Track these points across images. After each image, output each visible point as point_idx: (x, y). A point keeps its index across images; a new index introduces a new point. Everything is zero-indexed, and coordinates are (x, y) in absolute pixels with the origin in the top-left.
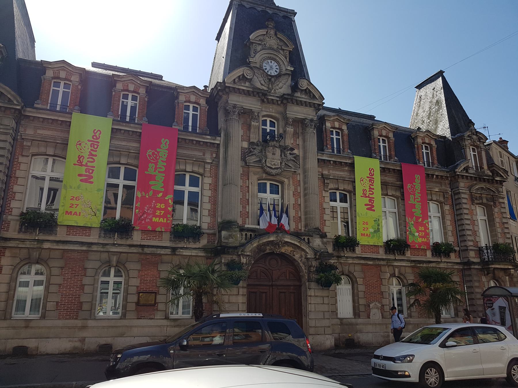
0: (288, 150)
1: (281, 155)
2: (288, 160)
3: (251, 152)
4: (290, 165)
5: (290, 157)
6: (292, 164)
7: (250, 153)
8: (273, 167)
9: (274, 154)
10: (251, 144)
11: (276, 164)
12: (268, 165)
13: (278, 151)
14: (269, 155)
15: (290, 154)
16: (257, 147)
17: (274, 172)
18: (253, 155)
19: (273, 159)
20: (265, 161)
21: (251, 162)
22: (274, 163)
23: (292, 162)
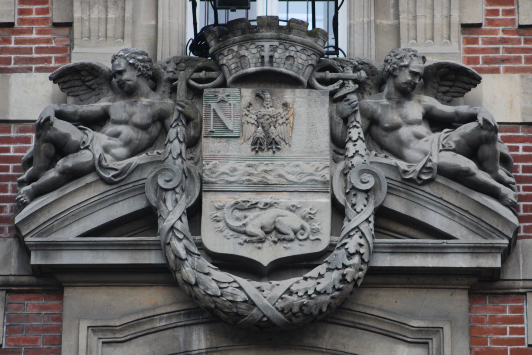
0: (405, 93)
1: (338, 144)
2: (410, 184)
3: (61, 148)
4: (436, 219)
5: (431, 148)
6: (450, 211)
7: (51, 163)
8: (265, 255)
9: (266, 144)
10: (77, 79)
11: (290, 222)
13: (307, 115)
14: (227, 159)
15: (435, 122)
16: (118, 108)
17: (268, 296)
18: (72, 175)
19: (264, 187)
20: (194, 213)
21: (71, 234)
22: (267, 217)
23: (451, 193)
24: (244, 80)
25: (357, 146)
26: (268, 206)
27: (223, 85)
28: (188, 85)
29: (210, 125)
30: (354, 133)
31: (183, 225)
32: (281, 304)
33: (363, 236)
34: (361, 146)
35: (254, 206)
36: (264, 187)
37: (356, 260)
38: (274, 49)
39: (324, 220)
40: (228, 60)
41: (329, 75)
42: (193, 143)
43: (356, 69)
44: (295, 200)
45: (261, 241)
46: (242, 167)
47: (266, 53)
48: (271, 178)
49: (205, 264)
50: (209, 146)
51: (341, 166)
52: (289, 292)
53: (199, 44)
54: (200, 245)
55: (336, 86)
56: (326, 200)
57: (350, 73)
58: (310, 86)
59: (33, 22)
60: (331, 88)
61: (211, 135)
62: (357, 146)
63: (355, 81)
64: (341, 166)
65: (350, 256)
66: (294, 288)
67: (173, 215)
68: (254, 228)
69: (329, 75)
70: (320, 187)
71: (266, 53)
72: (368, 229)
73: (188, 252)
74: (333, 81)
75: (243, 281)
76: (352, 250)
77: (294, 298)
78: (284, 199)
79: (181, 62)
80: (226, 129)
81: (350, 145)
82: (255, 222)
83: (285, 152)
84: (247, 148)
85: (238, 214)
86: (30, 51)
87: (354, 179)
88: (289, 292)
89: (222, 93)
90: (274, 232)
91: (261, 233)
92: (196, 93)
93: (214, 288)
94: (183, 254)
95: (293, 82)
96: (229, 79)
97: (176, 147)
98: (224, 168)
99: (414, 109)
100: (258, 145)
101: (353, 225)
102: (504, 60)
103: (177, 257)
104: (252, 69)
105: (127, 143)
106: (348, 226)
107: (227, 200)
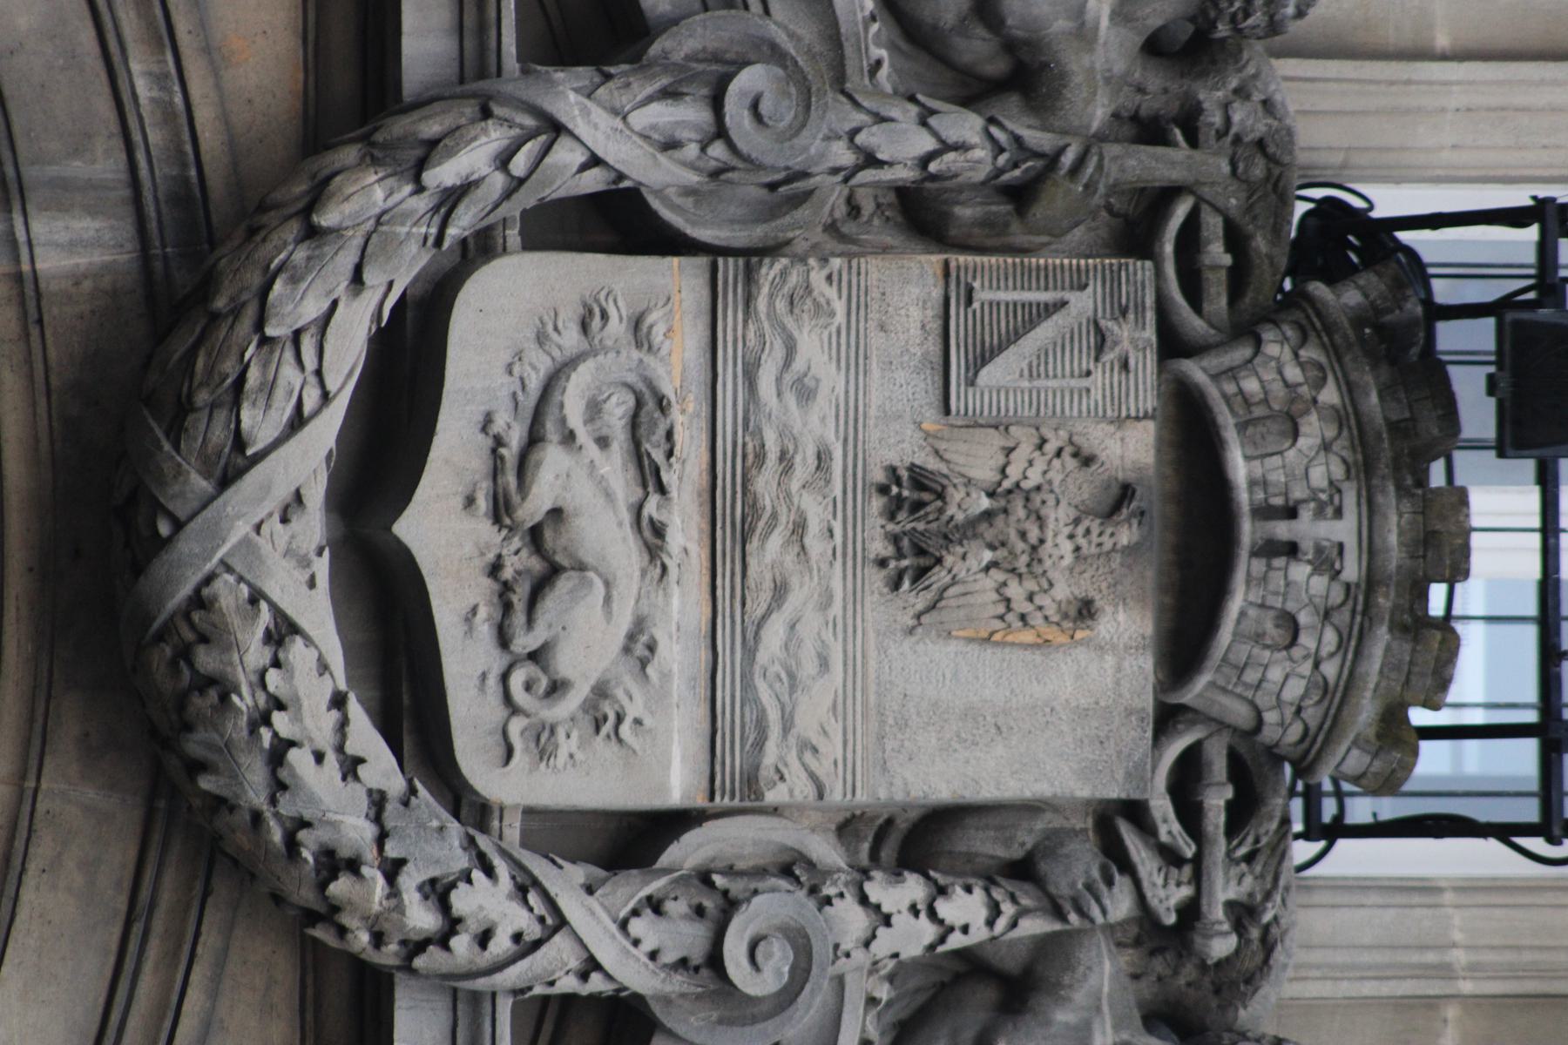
1: (920, 840)
8: (440, 529)
9: (919, 526)
11: (584, 635)
12: (504, 319)
14: (855, 359)
17: (265, 541)
19: (733, 523)
20: (618, 221)
22: (602, 532)
24: (1192, 432)
25: (908, 921)
26: (653, 536)
27: (1172, 344)
28: (1167, 195)
29: (996, 286)
30: (965, 909)
31: (565, 172)
32: (229, 594)
33: (525, 946)
34: (911, 937)
35: (650, 478)
36: (733, 523)
37: (421, 918)
38: (1327, 560)
39: (591, 781)
40: (1280, 362)
41: (1217, 800)
42: (921, 214)
43: (1242, 914)
44: (679, 656)
45: (501, 510)
46: (816, 425)
47: (1307, 529)
48: (770, 551)
49: (402, 270)
50: (908, 285)
51: (825, 850)
52: (283, 631)
53: (1350, 240)
54: (481, 248)
55: (1169, 827)
56: (677, 785)
57: (1224, 888)
58: (1167, 718)
60: (1162, 807)
61: (955, 294)
62: (908, 921)
63: (1190, 912)
64: (825, 850)
65: (438, 892)
66: (297, 652)
67: (613, 129)
69: (1217, 800)
70: (734, 761)
71: (1307, 529)
72: (554, 965)
73: (453, 197)
75: (326, 430)
76: (461, 901)
77: (256, 654)
78: (682, 608)
79: (1268, 161)
80: (983, 357)
81: (914, 888)
82: (582, 484)
83: (883, 611)
84: (897, 445)
85: (617, 410)
87: (770, 907)
88: (283, 631)
89: (1136, 338)
90: (540, 565)
91: (533, 508)
92: (1135, 225)
93: (297, 306)
94: (444, 174)
95: (1185, 642)
96: (1195, 371)
97: (904, 144)
98: (812, 347)
100: (913, 492)
101: (573, 906)
103: (429, 152)
104: (1239, 468)
106: (565, 882)
107: (677, 361)
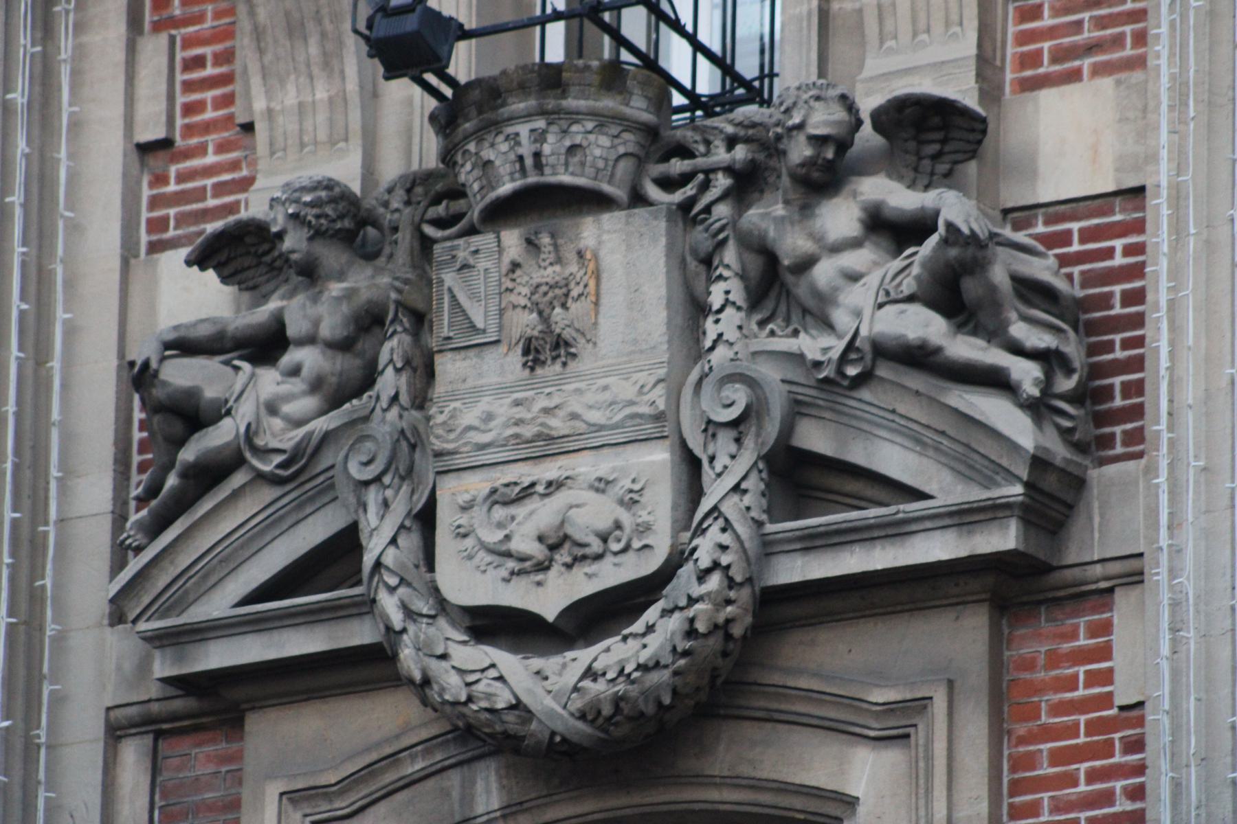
0: (824, 178)
4: (892, 458)
8: (550, 598)
9: (546, 349)
11: (592, 515)
14: (480, 393)
19: (546, 445)
21: (219, 603)
26: (554, 486)
32: (577, 703)
35: (527, 492)
36: (546, 445)
42: (423, 370)
45: (543, 567)
47: (526, 149)
48: (558, 424)
50: (449, 368)
52: (590, 673)
55: (689, 190)
59: (207, 127)
68: (525, 544)
70: (649, 428)
74: (685, 179)
77: (599, 687)
78: (586, 466)
86: (200, 194)
95: (590, 201)
98: (470, 417)
99: (840, 217)
102: (1092, 48)
105: (316, 385)
